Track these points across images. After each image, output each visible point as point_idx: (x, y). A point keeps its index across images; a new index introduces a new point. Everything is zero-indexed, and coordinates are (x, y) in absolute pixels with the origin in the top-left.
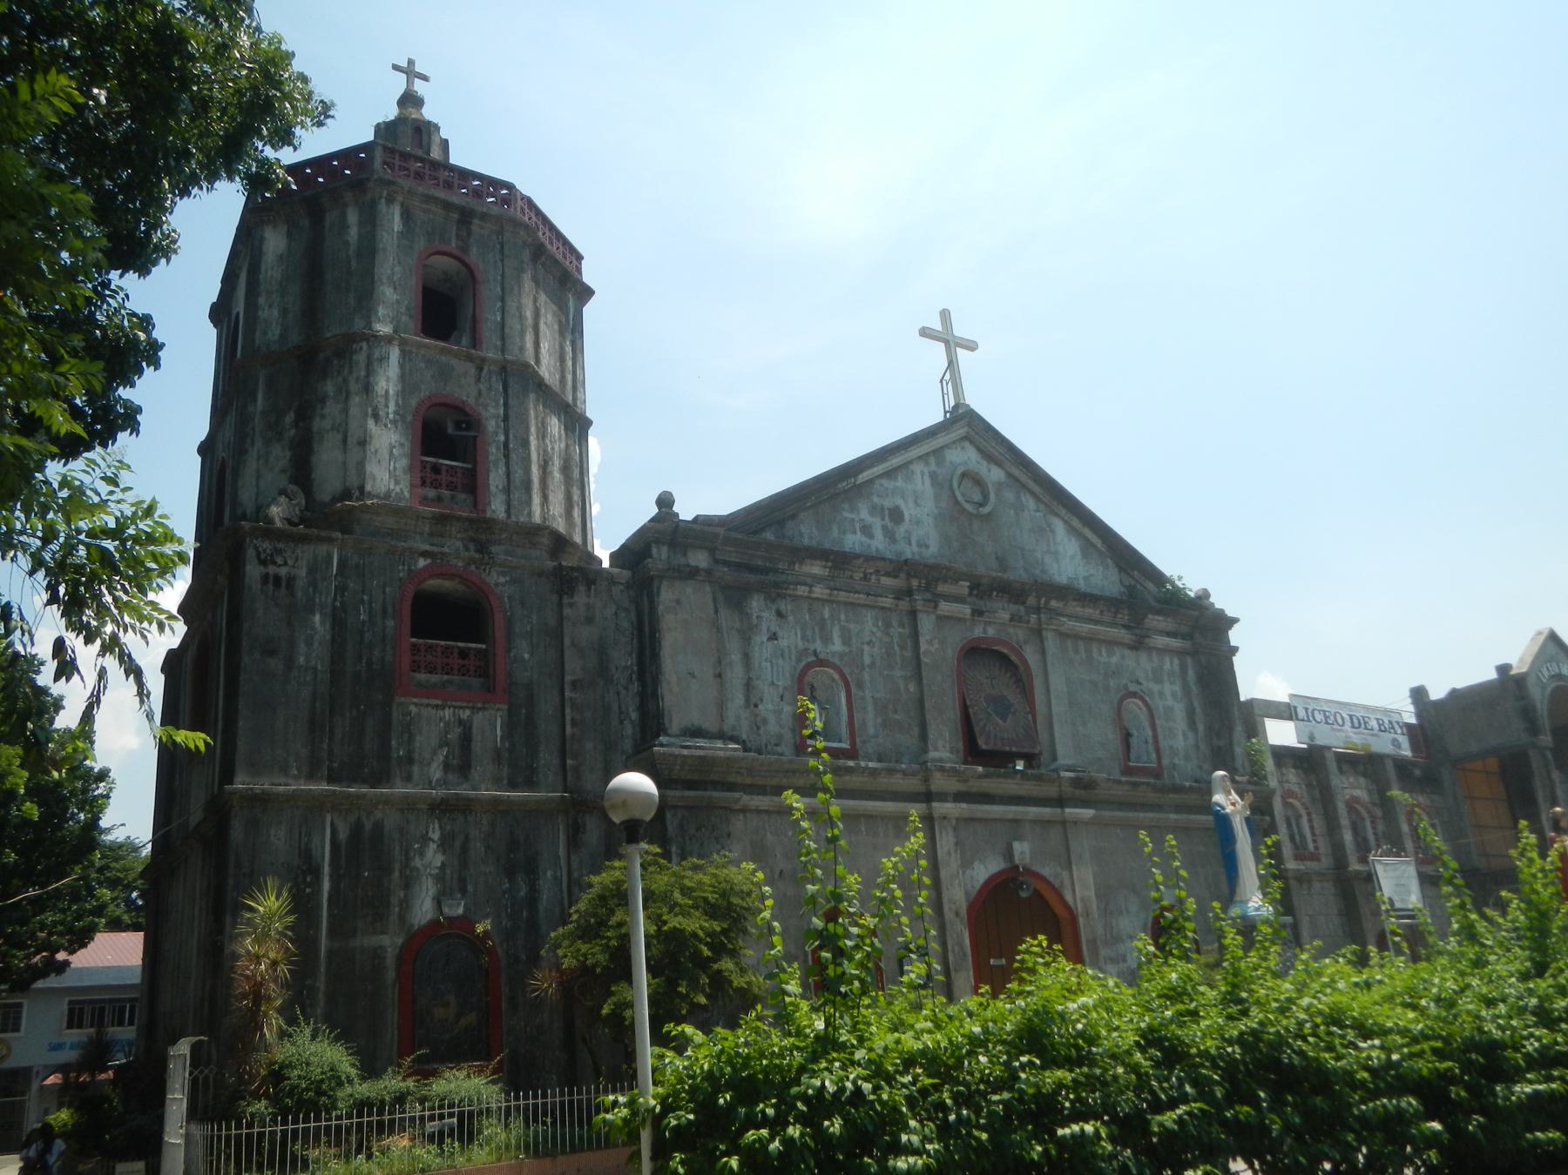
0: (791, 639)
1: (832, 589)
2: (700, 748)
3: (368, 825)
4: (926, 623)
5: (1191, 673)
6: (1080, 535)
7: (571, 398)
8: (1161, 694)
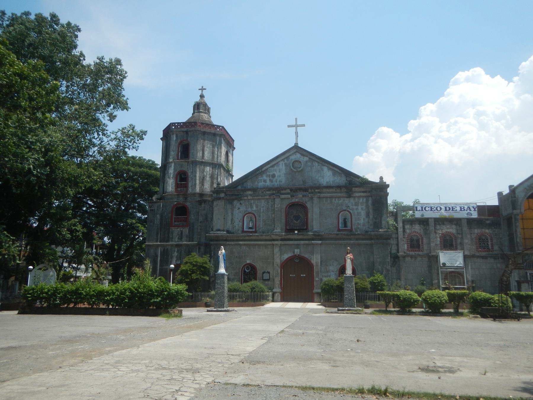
0: (243, 209)
1: (253, 197)
2: (217, 234)
3: (166, 249)
4: (277, 201)
5: (370, 202)
6: (332, 170)
7: (216, 160)
8: (357, 209)
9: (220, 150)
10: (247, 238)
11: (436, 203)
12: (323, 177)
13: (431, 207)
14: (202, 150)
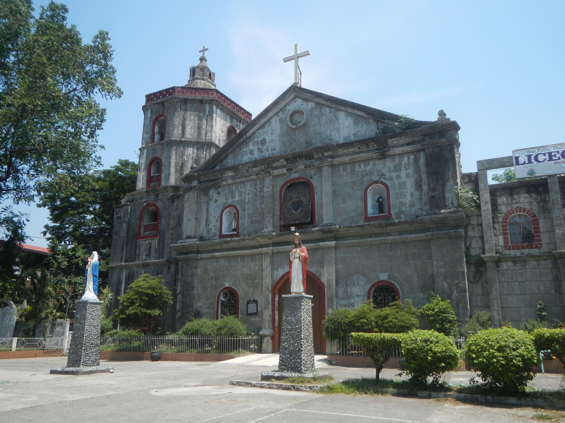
0: (221, 200)
3: (131, 271)
4: (268, 180)
5: (422, 160)
7: (204, 138)
8: (398, 177)
9: (210, 123)
10: (225, 246)
11: (560, 144)
12: (338, 130)
13: (550, 154)
14: (182, 125)
